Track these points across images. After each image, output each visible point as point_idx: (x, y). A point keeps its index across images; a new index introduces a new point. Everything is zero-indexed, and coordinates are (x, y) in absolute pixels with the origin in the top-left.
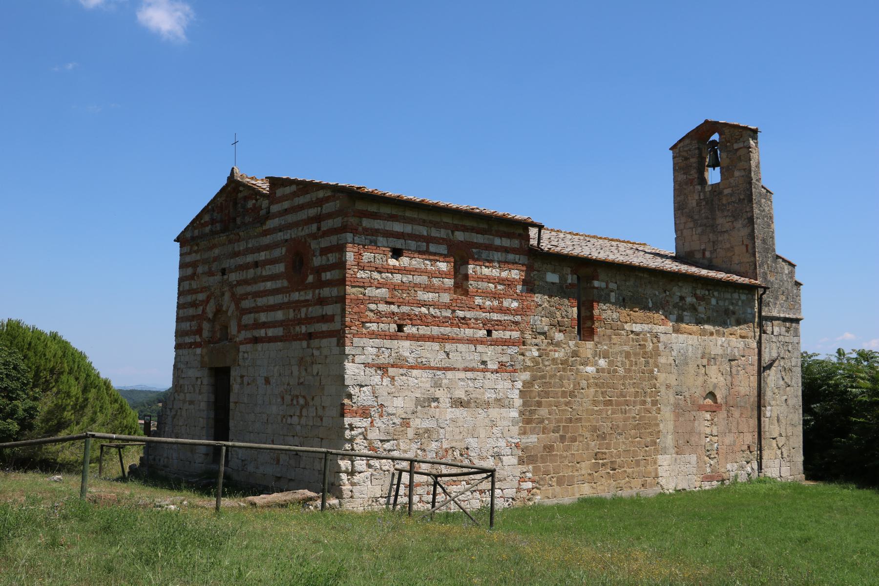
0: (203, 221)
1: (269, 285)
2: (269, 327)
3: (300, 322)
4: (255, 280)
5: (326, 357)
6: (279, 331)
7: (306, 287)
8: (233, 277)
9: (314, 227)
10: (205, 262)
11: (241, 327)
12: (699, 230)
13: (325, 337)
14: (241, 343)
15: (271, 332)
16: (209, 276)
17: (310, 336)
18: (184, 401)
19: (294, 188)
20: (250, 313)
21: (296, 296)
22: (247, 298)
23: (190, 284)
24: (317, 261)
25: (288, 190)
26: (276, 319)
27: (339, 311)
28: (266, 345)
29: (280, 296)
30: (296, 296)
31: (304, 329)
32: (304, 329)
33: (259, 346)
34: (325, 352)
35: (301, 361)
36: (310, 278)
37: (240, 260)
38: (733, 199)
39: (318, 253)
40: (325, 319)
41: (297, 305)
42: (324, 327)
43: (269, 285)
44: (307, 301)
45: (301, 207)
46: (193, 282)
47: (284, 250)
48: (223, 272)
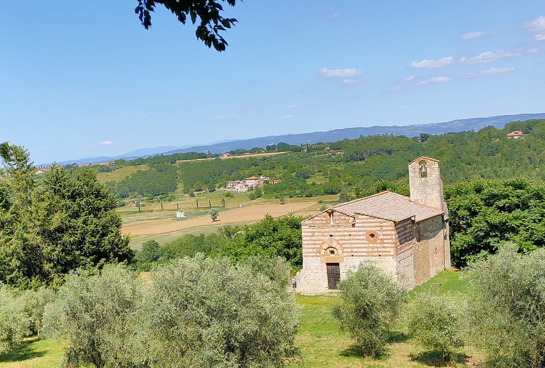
1: (358, 241)
5: (388, 261)
6: (365, 254)
7: (377, 243)
8: (337, 238)
9: (379, 228)
10: (319, 232)
11: (343, 252)
12: (420, 193)
14: (344, 256)
15: (360, 254)
17: (380, 255)
20: (349, 248)
21: (372, 245)
24: (381, 237)
25: (365, 217)
30: (372, 245)
31: (376, 254)
32: (376, 254)
33: (355, 257)
36: (378, 241)
37: (340, 234)
38: (432, 184)
40: (385, 252)
41: (372, 248)
45: (373, 222)
46: (312, 237)
47: (365, 233)
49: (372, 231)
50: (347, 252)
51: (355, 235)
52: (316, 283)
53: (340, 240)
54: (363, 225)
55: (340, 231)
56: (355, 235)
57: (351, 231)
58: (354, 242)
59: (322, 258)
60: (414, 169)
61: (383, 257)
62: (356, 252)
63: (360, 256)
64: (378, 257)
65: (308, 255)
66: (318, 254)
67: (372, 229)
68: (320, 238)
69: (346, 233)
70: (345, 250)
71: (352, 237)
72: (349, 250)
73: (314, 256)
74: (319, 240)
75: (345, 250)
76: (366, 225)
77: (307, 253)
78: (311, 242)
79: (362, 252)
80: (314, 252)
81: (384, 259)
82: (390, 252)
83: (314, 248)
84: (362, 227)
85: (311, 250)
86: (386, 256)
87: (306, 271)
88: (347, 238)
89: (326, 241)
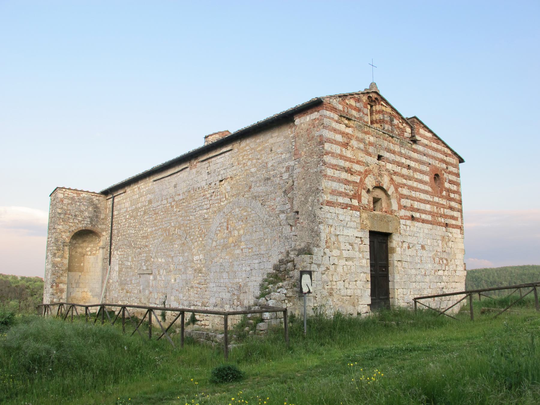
2: (422, 213)
3: (441, 216)
4: (409, 178)
5: (455, 238)
7: (442, 197)
9: (444, 166)
14: (402, 218)
15: (424, 216)
16: (366, 154)
17: (447, 225)
18: (340, 257)
20: (407, 198)
21: (436, 199)
22: (404, 187)
24: (447, 185)
27: (460, 216)
28: (420, 224)
29: (428, 196)
30: (436, 199)
33: (416, 224)
34: (455, 236)
36: (444, 193)
39: (447, 181)
40: (453, 218)
41: (437, 205)
42: (453, 222)
48: (380, 157)
49: (437, 168)
50: (405, 207)
51: (415, 170)
52: (349, 292)
53: (395, 173)
56: (415, 170)
62: (418, 210)
64: (444, 229)
66: (355, 202)
68: (362, 157)
69: (403, 160)
70: (404, 202)
74: (358, 162)
75: (404, 202)
76: (430, 152)
77: (333, 192)
78: (342, 163)
79: (424, 212)
80: (347, 195)
83: (347, 182)
84: (425, 155)
85: (342, 188)
87: (327, 251)
88: (405, 171)
89: (371, 167)
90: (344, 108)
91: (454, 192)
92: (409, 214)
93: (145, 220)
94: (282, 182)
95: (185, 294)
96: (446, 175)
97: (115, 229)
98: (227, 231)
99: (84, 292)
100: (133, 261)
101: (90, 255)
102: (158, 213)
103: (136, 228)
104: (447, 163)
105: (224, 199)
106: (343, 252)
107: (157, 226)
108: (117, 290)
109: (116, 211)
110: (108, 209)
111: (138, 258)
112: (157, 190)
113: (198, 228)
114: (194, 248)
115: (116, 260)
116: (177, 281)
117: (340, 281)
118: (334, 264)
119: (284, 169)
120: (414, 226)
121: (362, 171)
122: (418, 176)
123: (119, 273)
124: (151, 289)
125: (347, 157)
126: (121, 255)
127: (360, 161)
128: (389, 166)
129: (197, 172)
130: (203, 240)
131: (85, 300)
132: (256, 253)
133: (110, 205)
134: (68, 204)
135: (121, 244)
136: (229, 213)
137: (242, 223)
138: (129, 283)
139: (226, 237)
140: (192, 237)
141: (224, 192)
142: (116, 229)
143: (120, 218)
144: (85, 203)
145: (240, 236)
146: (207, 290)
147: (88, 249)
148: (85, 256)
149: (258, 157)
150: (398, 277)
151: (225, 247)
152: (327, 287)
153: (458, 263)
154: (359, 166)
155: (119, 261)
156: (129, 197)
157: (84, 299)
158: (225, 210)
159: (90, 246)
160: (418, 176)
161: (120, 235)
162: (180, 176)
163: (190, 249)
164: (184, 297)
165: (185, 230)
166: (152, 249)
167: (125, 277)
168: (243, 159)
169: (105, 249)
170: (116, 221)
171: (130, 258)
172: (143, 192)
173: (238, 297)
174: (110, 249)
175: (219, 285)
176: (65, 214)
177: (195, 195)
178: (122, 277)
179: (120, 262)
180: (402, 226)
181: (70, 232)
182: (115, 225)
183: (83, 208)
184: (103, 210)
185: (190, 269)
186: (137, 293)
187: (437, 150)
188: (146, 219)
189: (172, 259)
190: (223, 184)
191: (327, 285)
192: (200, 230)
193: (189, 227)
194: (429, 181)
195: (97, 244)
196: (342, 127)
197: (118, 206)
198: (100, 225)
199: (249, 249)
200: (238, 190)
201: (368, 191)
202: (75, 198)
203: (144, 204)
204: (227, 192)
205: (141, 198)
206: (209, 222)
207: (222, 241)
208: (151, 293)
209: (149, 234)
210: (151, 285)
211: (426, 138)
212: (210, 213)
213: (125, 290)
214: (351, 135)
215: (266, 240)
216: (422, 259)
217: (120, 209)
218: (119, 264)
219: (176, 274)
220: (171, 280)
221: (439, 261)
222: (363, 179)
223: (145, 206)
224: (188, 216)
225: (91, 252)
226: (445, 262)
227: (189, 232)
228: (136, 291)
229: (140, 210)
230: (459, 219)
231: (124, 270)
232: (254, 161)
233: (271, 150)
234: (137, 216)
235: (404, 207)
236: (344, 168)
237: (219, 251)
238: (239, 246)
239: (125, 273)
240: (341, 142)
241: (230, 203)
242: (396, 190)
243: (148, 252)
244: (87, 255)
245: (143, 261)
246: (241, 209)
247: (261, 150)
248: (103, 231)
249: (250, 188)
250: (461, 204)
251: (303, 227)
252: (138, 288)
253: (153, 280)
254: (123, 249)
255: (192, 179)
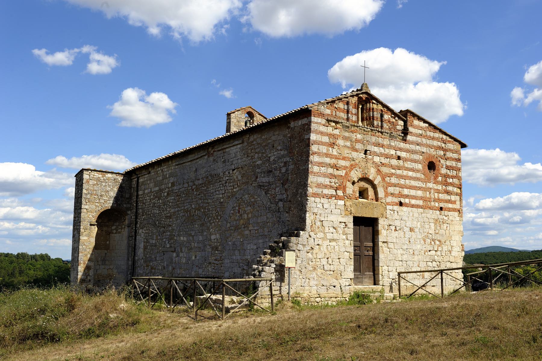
0: (335, 105)
1: (410, 174)
3: (435, 200)
5: (452, 221)
6: (420, 203)
8: (377, 159)
9: (442, 153)
10: (345, 138)
11: (387, 194)
13: (451, 211)
14: (388, 204)
15: (413, 202)
17: (441, 209)
19: (427, 125)
20: (395, 186)
23: (328, 150)
24: (444, 171)
26: (417, 195)
29: (420, 183)
30: (430, 185)
31: (437, 205)
33: (404, 209)
35: (436, 221)
36: (440, 179)
40: (449, 201)
42: (450, 206)
43: (410, 174)
44: (439, 190)
51: (406, 160)
52: (332, 268)
53: (383, 164)
54: (419, 140)
55: (383, 146)
56: (406, 160)
57: (401, 149)
58: (405, 173)
59: (348, 203)
60: (238, 122)
61: (446, 213)
62: (407, 196)
63: (413, 206)
64: (438, 212)
65: (319, 191)
66: (340, 193)
67: (432, 152)
69: (393, 152)
70: (391, 189)
71: (401, 162)
72: (397, 190)
73: (331, 196)
74: (344, 159)
75: (391, 189)
77: (319, 186)
78: (327, 160)
80: (331, 187)
81: (446, 218)
82: (454, 202)
83: (332, 176)
84: (418, 145)
85: (326, 181)
86: (449, 210)
88: (394, 162)
89: (357, 161)
90: (332, 112)
91: (453, 177)
92: (396, 200)
93: (168, 201)
94: (280, 175)
95: (204, 270)
96: (442, 161)
97: (140, 209)
98: (239, 215)
99: (110, 269)
100: (157, 239)
101: (116, 233)
102: (180, 196)
103: (160, 208)
104: (445, 150)
105: (236, 186)
106: (327, 234)
107: (179, 207)
108: (142, 267)
109: (140, 191)
110: (132, 188)
111: (162, 237)
112: (179, 174)
113: (215, 211)
114: (212, 228)
115: (141, 239)
116: (198, 258)
117: (324, 258)
118: (318, 245)
119: (282, 165)
120: (402, 211)
121: (348, 165)
122: (408, 165)
123: (144, 250)
124: (174, 265)
125: (333, 155)
126: (146, 233)
127: (345, 157)
128: (377, 159)
129: (214, 160)
130: (219, 222)
131: (110, 277)
132: (261, 234)
133: (134, 184)
134: (94, 185)
135: (146, 223)
136: (241, 198)
137: (250, 208)
138: (154, 259)
139: (238, 220)
140: (210, 219)
141: (236, 180)
142: (141, 208)
143: (145, 198)
144: (110, 183)
145: (248, 219)
146: (223, 265)
147: (113, 228)
148: (111, 234)
149: (263, 152)
150: (383, 256)
151: (237, 228)
152: (311, 263)
153: (455, 244)
154: (344, 161)
155: (144, 239)
156: (153, 178)
157: (110, 276)
158: (237, 196)
159: (115, 224)
160: (408, 165)
161: (145, 214)
162: (199, 162)
163: (208, 229)
164: (203, 272)
165: (204, 212)
166: (175, 228)
167: (150, 254)
168: (252, 152)
169: (130, 228)
170: (142, 201)
171: (155, 236)
172: (166, 174)
173: (247, 271)
174: (136, 227)
175: (232, 261)
176: (91, 194)
177: (212, 181)
178: (147, 254)
179: (145, 240)
180: (388, 212)
181: (96, 212)
182: (139, 204)
183: (108, 189)
184: (127, 189)
185: (208, 247)
186: (162, 270)
187: (433, 138)
188: (170, 200)
189: (193, 238)
190: (235, 173)
191: (312, 262)
192: (217, 213)
193: (207, 209)
194: (421, 168)
195: (123, 222)
196: (330, 130)
197: (143, 186)
198: (125, 204)
199: (256, 230)
200: (247, 179)
201: (353, 183)
202: (101, 178)
203: (168, 186)
204: (239, 180)
205: (164, 180)
206: (224, 205)
207: (235, 223)
208: (174, 269)
209: (172, 214)
210: (174, 262)
211: (421, 128)
212: (225, 198)
213: (150, 267)
214: (337, 135)
215: (268, 224)
216: (410, 241)
217: (145, 189)
218: (144, 242)
219: (196, 251)
220: (192, 257)
221: (431, 242)
222: (349, 172)
223: (168, 188)
224: (207, 199)
225: (117, 230)
226: (437, 243)
227: (208, 214)
228: (160, 268)
229: (164, 191)
230: (458, 203)
231: (149, 247)
232: (260, 155)
233: (273, 147)
234: (161, 197)
235: (391, 194)
236: (330, 164)
237: (232, 231)
238: (248, 228)
239: (149, 251)
240: (328, 143)
241: (241, 189)
242: (383, 179)
243: (171, 231)
244: (113, 233)
245: (167, 239)
246: (249, 196)
247: (265, 146)
248: (128, 210)
249: (257, 178)
250: (460, 188)
251: (294, 214)
252: (162, 264)
253: (176, 257)
254: (148, 228)
255: (210, 166)
